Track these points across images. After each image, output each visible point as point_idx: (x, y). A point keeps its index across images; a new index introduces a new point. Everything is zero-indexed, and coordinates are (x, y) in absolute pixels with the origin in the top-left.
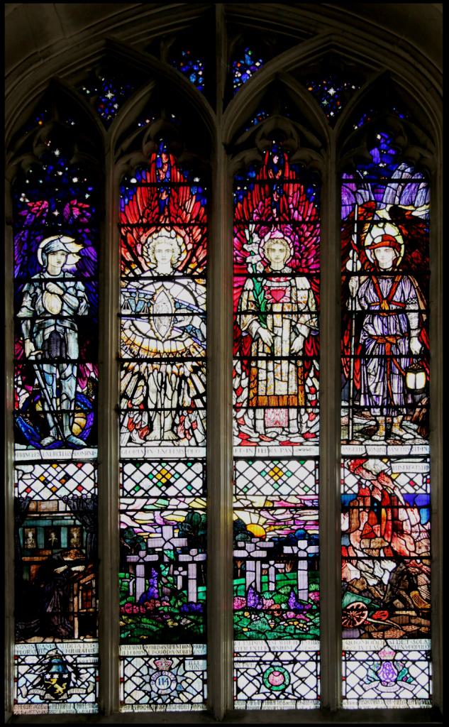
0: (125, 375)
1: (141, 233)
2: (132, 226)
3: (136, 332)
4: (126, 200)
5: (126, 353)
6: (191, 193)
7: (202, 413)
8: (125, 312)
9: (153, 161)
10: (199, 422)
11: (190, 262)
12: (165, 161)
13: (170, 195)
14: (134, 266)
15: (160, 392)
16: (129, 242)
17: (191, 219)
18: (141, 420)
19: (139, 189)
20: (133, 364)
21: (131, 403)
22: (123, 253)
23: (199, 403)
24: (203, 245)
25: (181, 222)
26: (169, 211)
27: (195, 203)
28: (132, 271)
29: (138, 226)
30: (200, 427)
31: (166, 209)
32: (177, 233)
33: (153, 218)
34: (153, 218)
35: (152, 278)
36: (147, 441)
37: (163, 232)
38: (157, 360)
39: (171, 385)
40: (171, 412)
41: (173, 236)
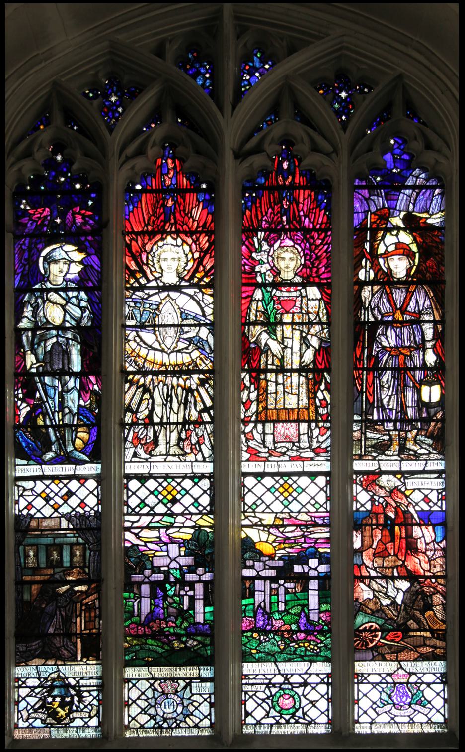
0: (129, 388)
1: (146, 241)
2: (137, 234)
3: (141, 343)
4: (131, 207)
5: (131, 365)
6: (198, 200)
7: (210, 428)
8: (129, 323)
9: (159, 167)
10: (206, 436)
11: (196, 271)
12: (171, 166)
13: (176, 202)
14: (138, 275)
15: (166, 406)
16: (133, 250)
17: (198, 227)
18: (146, 435)
19: (144, 195)
20: (137, 377)
21: (136, 417)
22: (127, 262)
23: (206, 417)
24: (211, 254)
25: (187, 230)
26: (175, 218)
27: (202, 209)
28: (137, 280)
29: (142, 233)
30: (207, 441)
31: (172, 217)
32: (184, 241)
33: (158, 226)
34: (158, 226)
35: (158, 287)
36: (152, 456)
37: (169, 240)
38: (162, 372)
39: (178, 399)
40: (177, 426)
41: (179, 244)
